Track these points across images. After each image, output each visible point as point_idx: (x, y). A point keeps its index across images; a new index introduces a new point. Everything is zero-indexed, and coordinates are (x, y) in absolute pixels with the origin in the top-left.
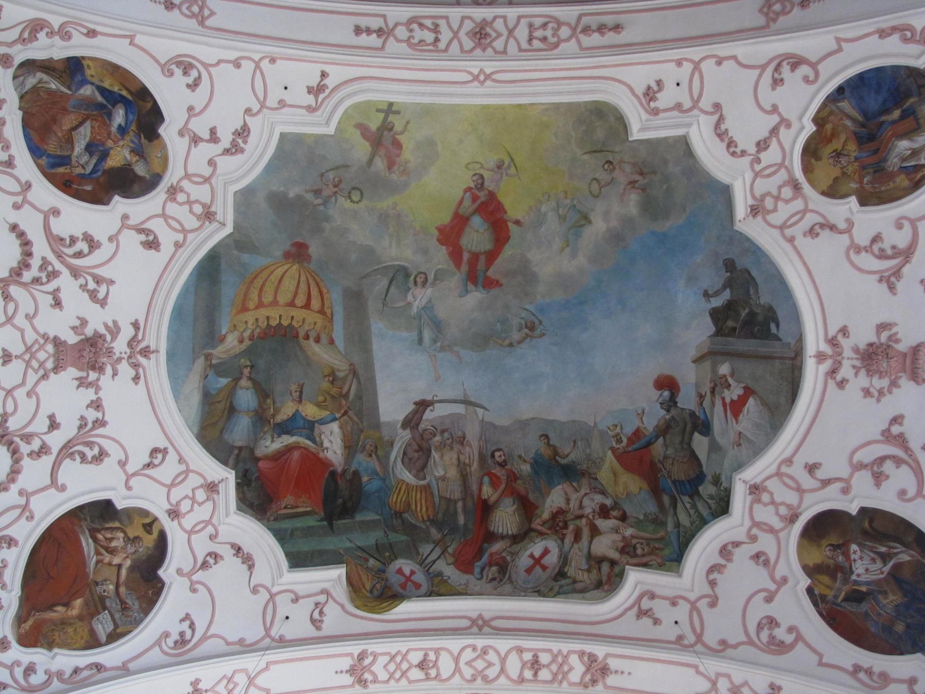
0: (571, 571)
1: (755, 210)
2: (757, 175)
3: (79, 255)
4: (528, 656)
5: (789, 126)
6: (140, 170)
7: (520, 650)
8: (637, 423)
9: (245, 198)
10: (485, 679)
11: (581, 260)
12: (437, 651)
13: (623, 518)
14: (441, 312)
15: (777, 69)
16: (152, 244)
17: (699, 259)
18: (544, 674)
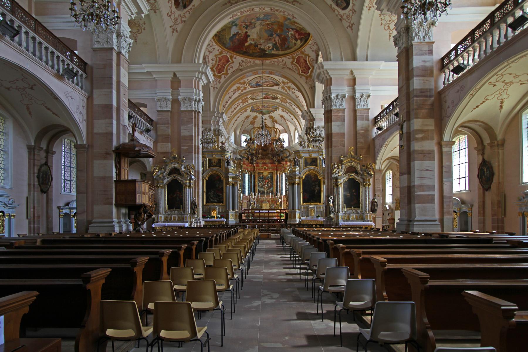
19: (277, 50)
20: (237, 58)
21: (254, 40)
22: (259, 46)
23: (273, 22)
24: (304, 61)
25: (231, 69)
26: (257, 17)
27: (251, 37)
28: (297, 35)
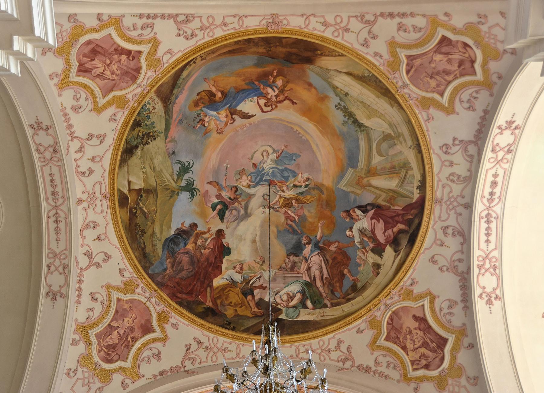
19: (315, 308)
20: (181, 326)
21: (242, 269)
22: (255, 292)
23: (302, 189)
24: (416, 325)
25: (153, 361)
26: (255, 165)
27: (234, 256)
28: (380, 226)
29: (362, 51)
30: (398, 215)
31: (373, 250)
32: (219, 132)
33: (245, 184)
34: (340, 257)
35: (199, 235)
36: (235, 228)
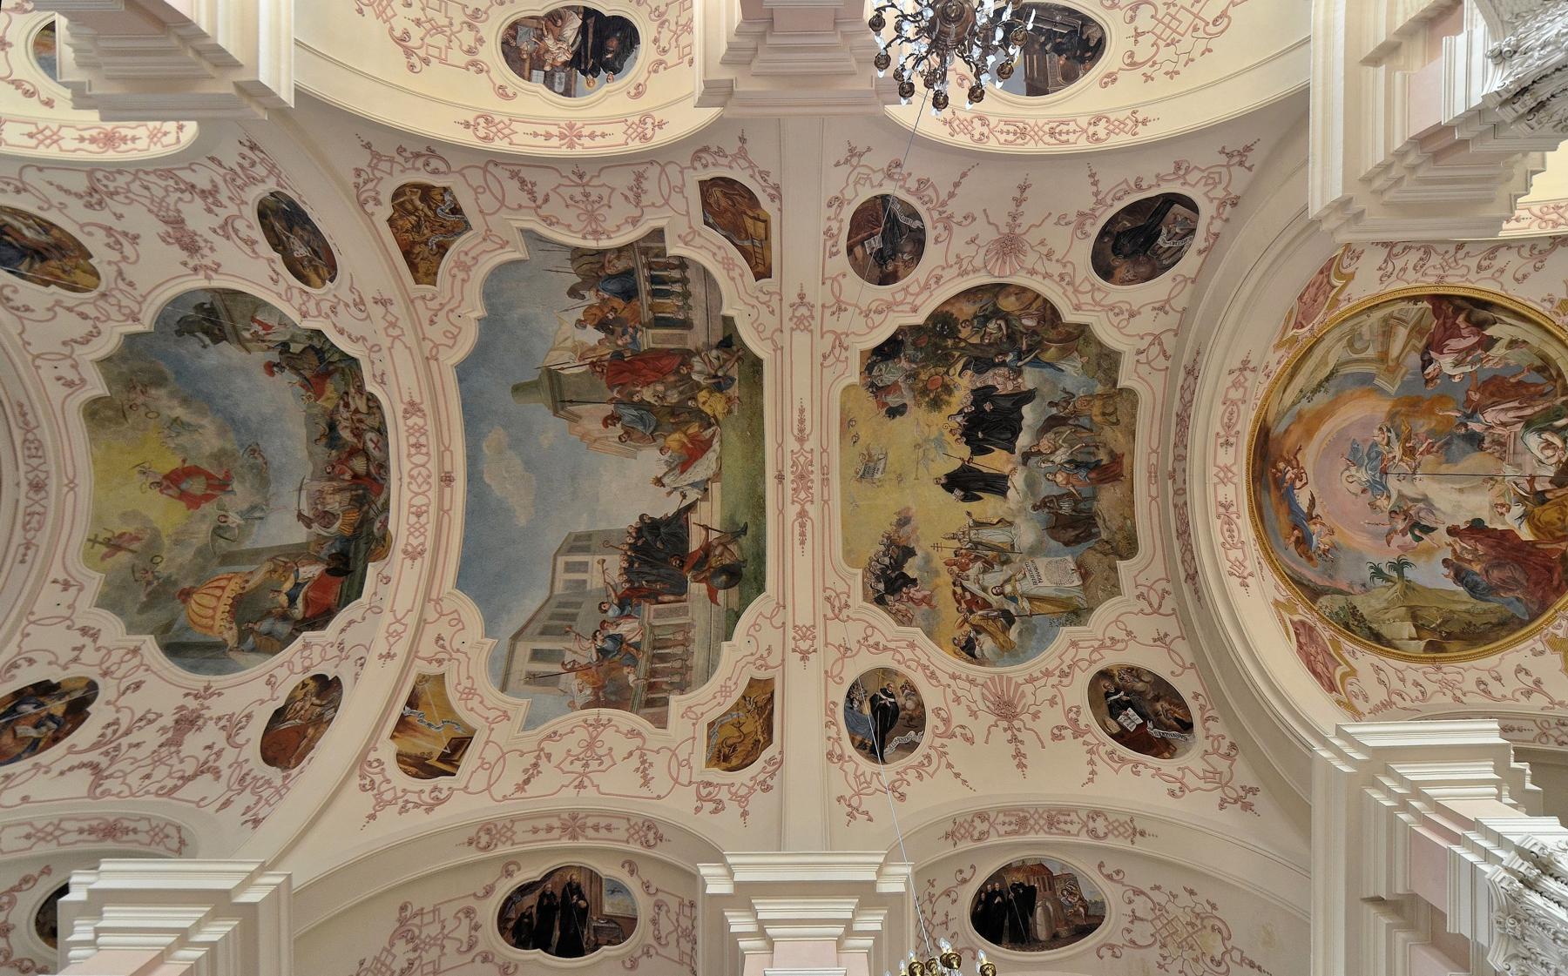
0: (377, 425)
1: (136, 320)
2: (109, 319)
3: (115, 732)
4: (413, 451)
5: (58, 303)
6: (77, 695)
7: (409, 456)
8: (298, 387)
9: (132, 628)
10: (429, 477)
11: (205, 422)
12: (411, 506)
13: (347, 393)
14: (246, 506)
15: (18, 309)
16: (138, 686)
17: (183, 352)
18: (423, 440)
21: (1503, 505)
22: (1539, 488)
23: (1393, 435)
26: (1364, 491)
27: (1485, 515)
28: (1455, 343)
29: (1273, 376)
30: (1444, 323)
31: (1487, 349)
32: (1332, 532)
33: (1386, 502)
34: (1491, 388)
35: (1458, 557)
36: (1444, 513)
